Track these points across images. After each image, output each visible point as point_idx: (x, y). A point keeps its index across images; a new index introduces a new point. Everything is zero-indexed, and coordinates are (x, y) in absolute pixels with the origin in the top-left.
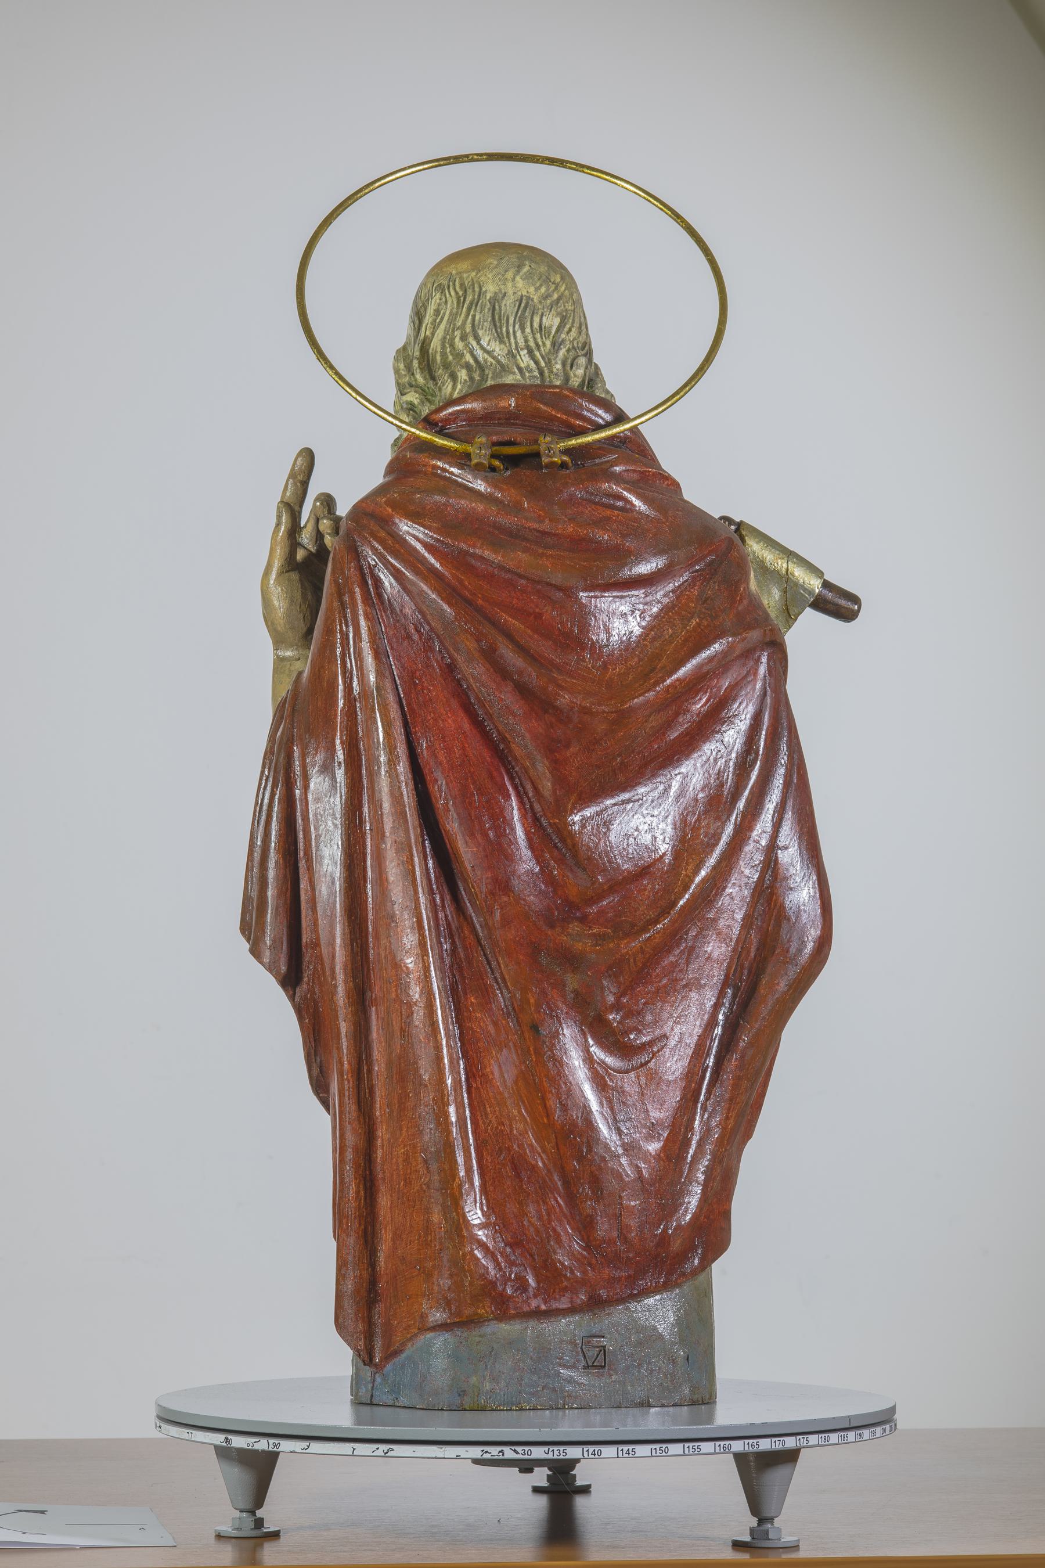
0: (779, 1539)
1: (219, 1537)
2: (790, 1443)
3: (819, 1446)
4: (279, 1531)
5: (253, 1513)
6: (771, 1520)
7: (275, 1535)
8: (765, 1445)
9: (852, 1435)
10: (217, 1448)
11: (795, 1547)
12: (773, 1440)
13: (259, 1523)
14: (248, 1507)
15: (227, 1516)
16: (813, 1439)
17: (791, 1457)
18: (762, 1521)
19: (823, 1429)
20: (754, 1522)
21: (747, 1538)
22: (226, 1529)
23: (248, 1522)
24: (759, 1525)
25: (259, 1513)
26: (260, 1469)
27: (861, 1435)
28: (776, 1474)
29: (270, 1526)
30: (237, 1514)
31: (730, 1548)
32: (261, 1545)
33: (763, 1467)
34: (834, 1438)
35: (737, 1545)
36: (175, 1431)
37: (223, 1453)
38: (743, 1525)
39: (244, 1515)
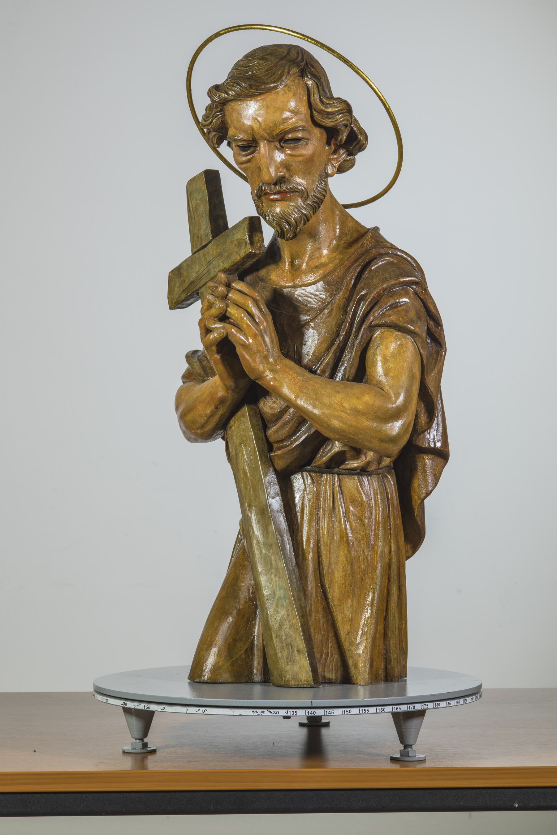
0: (415, 756)
1: (124, 752)
2: (418, 707)
3: (434, 708)
4: (156, 750)
5: (142, 740)
6: (411, 746)
7: (154, 752)
8: (404, 708)
9: (453, 703)
10: (123, 707)
11: (423, 761)
12: (408, 706)
13: (145, 745)
14: (140, 737)
15: (129, 742)
16: (431, 705)
17: (422, 713)
18: (406, 747)
19: (436, 699)
20: (402, 747)
21: (398, 756)
22: (128, 748)
23: (139, 744)
24: (404, 749)
25: (145, 740)
26: (146, 718)
27: (458, 702)
28: (414, 723)
29: (151, 747)
30: (134, 740)
31: (389, 761)
32: (146, 757)
33: (405, 721)
34: (442, 704)
35: (393, 759)
36: (100, 698)
37: (127, 711)
38: (396, 749)
39: (138, 741)
